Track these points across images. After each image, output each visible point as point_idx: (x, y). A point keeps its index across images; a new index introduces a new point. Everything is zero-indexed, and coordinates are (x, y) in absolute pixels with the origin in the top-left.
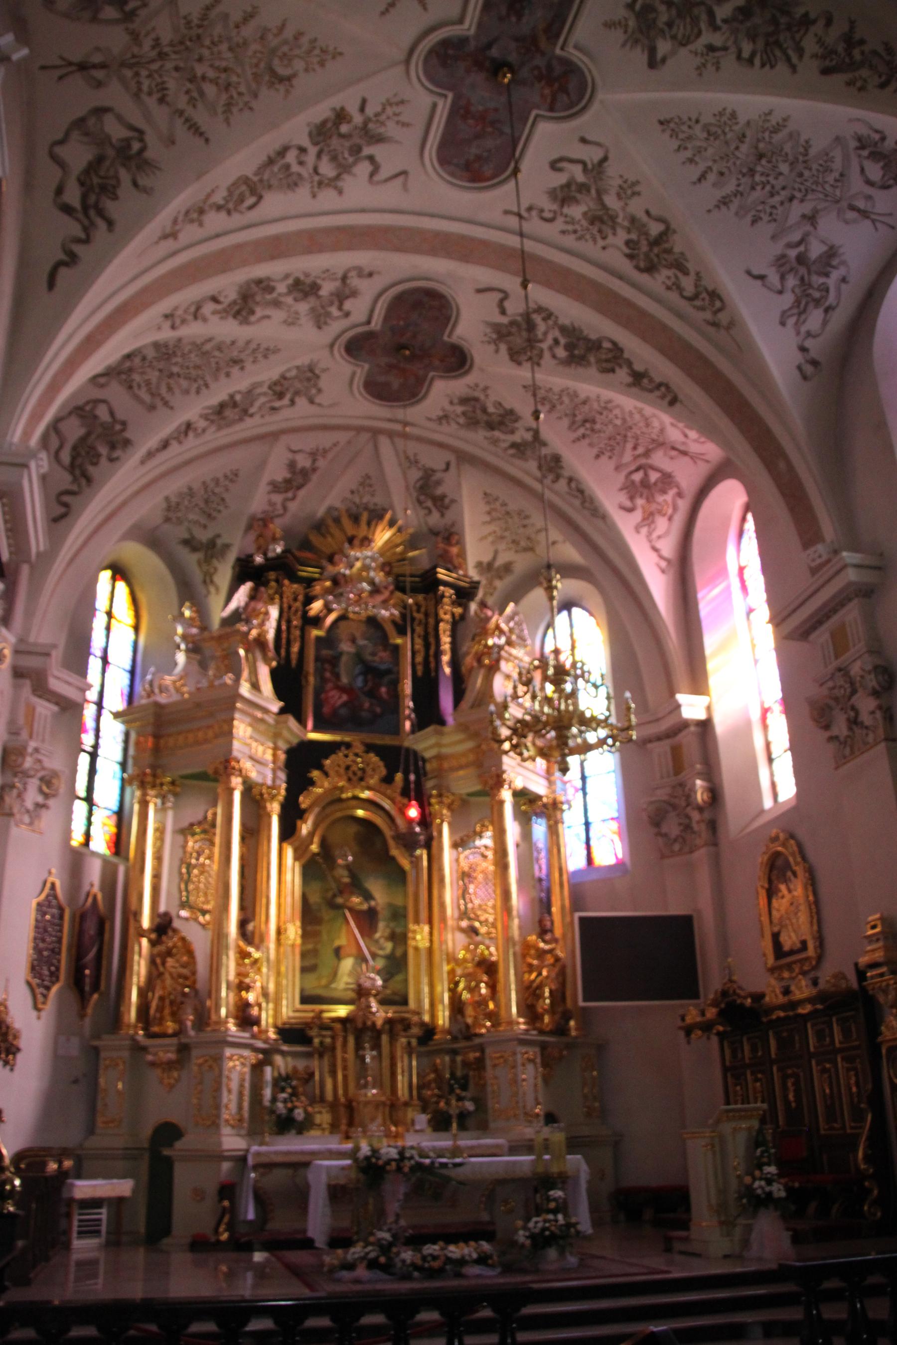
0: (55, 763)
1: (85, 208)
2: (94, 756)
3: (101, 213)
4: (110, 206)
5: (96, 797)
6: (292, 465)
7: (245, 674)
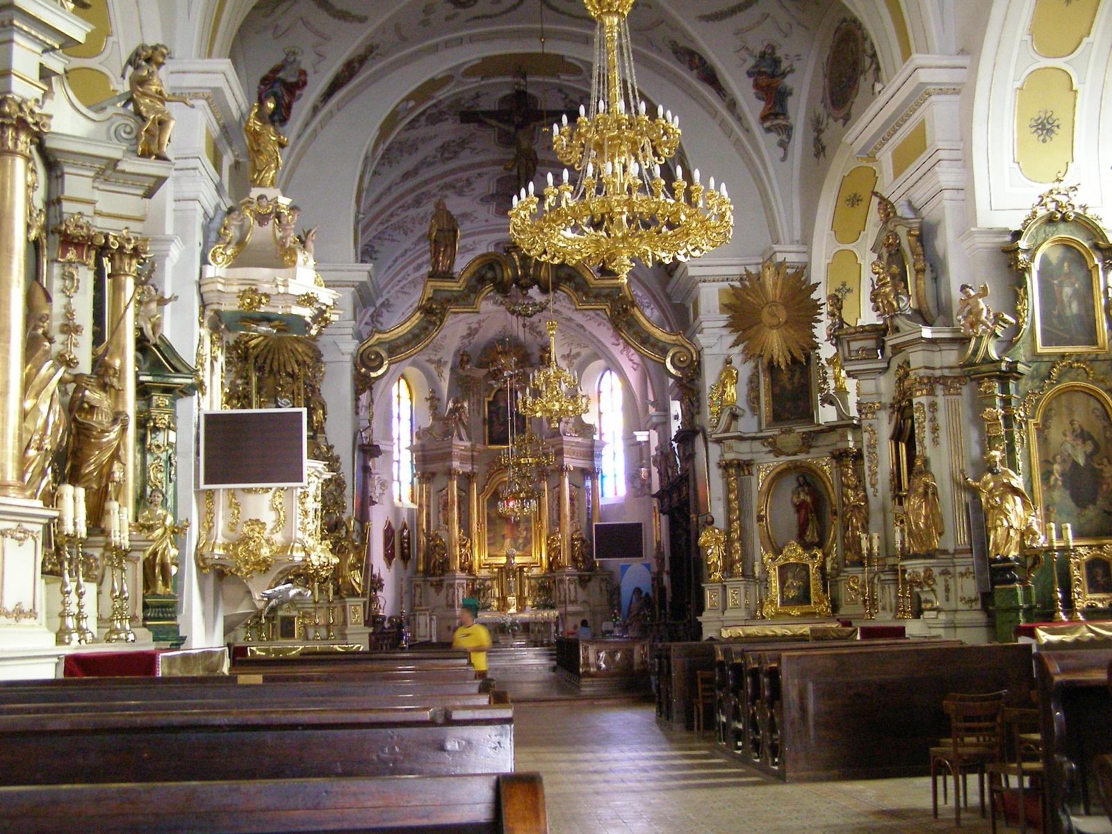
0: (384, 477)
1: (373, 322)
2: (398, 462)
3: (378, 322)
4: (380, 319)
5: (401, 479)
6: (470, 328)
7: (455, 433)
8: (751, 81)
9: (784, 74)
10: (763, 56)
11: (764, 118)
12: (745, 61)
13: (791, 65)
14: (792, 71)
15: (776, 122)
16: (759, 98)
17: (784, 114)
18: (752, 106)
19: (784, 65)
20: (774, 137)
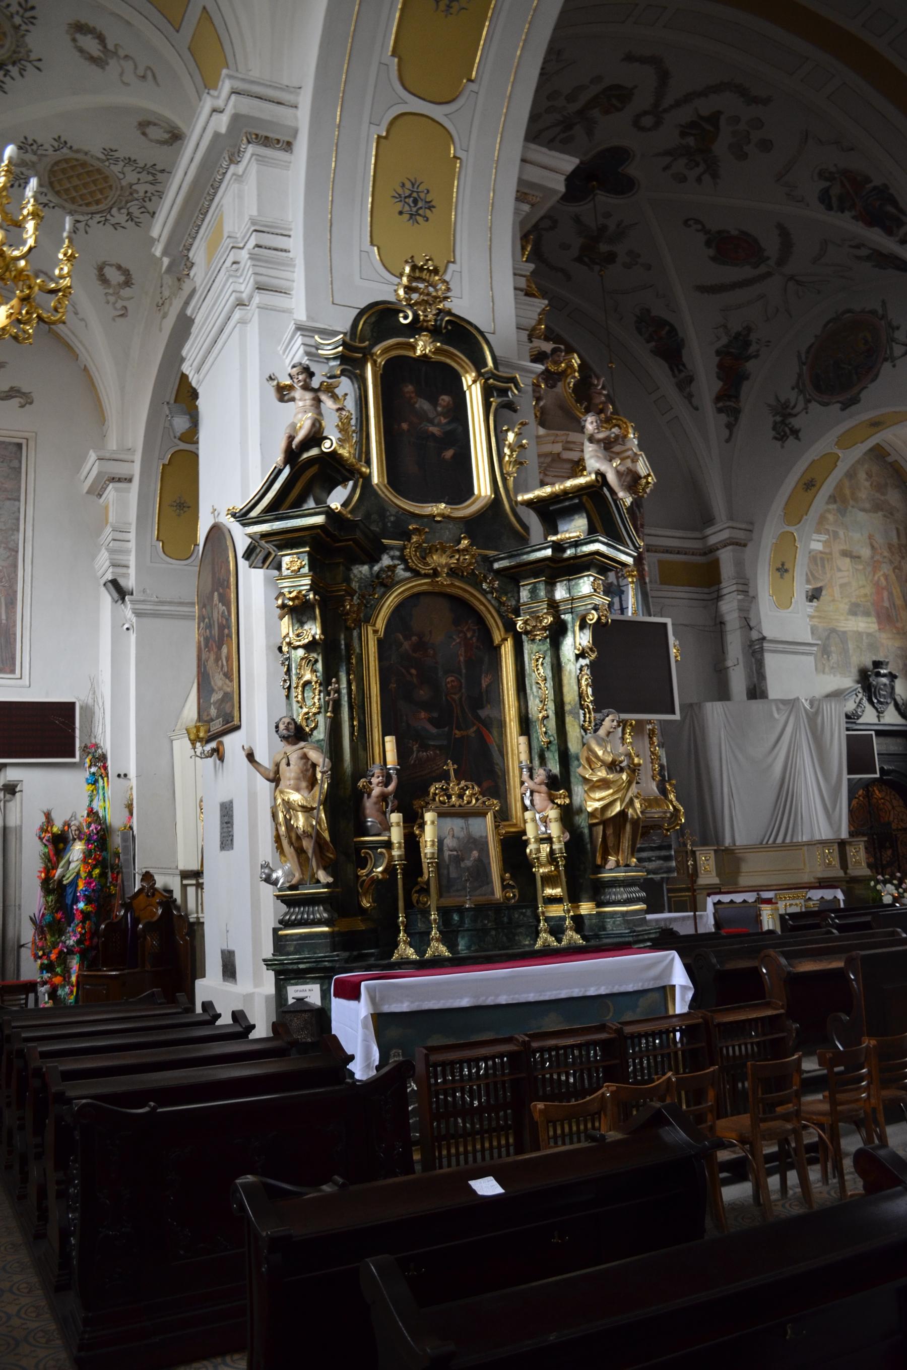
8: (717, 359)
9: (749, 358)
10: (738, 334)
11: (718, 399)
12: (719, 338)
13: (758, 351)
14: (756, 356)
15: (728, 403)
16: (719, 378)
17: (737, 397)
18: (707, 384)
19: (752, 349)
20: (723, 418)
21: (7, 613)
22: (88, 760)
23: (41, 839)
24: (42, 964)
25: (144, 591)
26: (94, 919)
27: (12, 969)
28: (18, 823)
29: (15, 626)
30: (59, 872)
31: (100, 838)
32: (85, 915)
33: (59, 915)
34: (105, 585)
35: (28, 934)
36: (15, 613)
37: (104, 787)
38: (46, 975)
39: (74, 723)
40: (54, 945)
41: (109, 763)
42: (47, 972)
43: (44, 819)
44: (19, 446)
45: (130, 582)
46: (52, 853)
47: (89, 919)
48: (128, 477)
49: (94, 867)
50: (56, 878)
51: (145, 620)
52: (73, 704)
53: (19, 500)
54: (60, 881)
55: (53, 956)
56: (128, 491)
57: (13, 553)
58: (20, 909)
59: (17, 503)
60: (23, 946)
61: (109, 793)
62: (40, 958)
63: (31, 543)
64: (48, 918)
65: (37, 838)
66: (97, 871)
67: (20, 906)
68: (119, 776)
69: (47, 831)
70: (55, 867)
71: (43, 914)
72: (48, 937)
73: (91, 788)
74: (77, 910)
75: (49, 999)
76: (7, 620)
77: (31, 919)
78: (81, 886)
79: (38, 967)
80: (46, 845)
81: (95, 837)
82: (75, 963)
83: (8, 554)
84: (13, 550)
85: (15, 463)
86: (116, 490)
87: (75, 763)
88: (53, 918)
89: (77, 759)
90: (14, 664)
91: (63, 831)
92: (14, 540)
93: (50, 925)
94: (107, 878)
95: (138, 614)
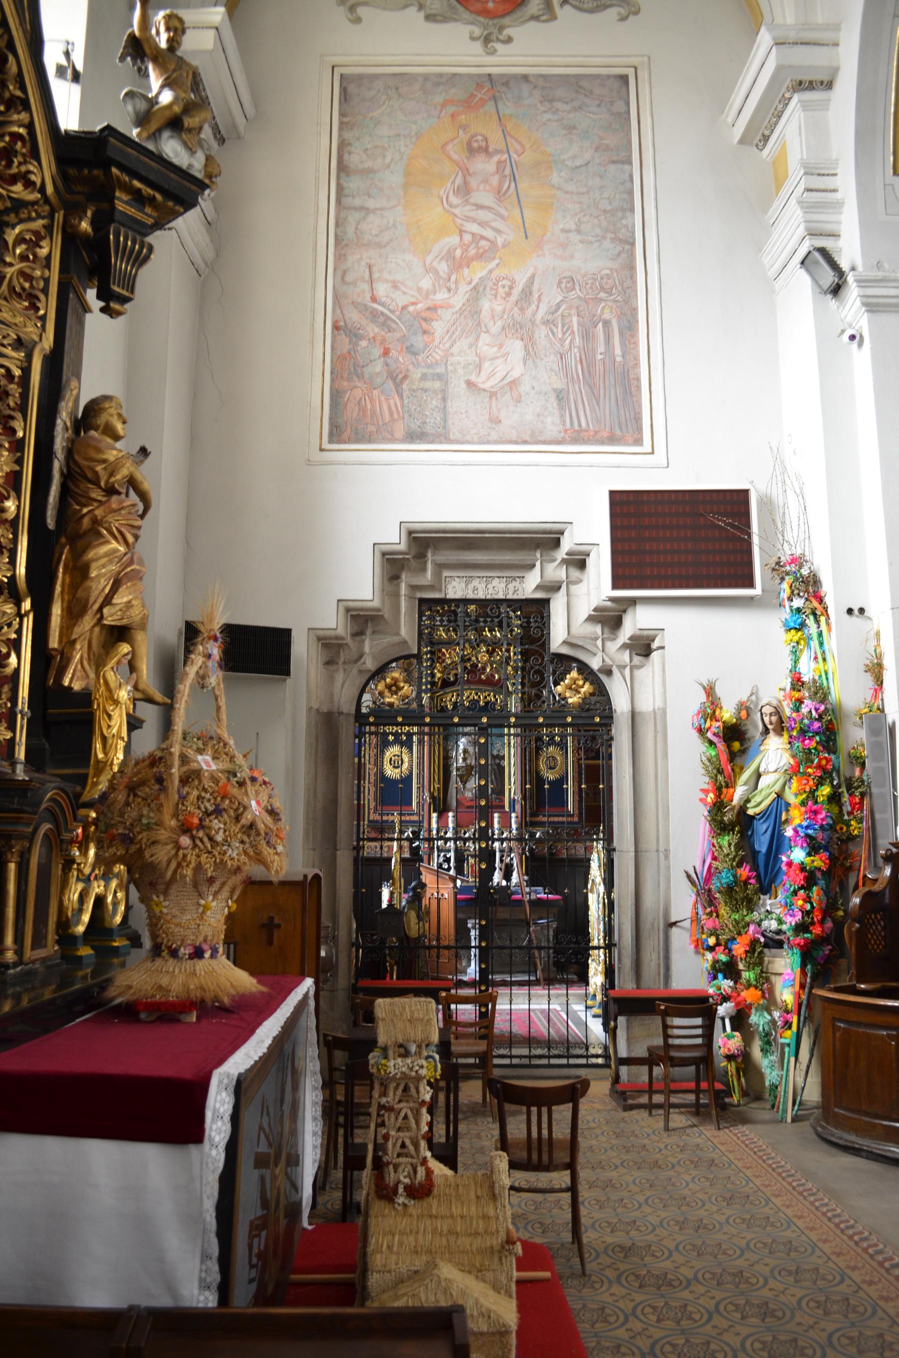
21: (623, 344)
22: (785, 586)
23: (701, 731)
24: (716, 962)
25: (879, 266)
26: (822, 883)
27: (654, 964)
28: (659, 704)
29: (637, 365)
30: (739, 793)
31: (820, 731)
32: (810, 878)
33: (744, 872)
34: (802, 263)
35: (683, 903)
36: (636, 344)
37: (820, 634)
38: (726, 984)
39: (748, 525)
40: (741, 927)
41: (828, 589)
42: (725, 977)
43: (703, 698)
44: (624, 79)
45: (850, 251)
46: (724, 757)
47: (816, 884)
48: (826, 79)
49: (820, 783)
50: (736, 801)
51: (886, 319)
52: (745, 493)
53: (630, 163)
54: (743, 809)
55: (739, 949)
56: (825, 106)
57: (627, 247)
58: (667, 857)
59: (627, 167)
60: (674, 924)
61: (832, 643)
62: (711, 949)
63: (654, 228)
64: (726, 878)
65: (695, 734)
66: (826, 790)
67: (667, 851)
68: (850, 611)
69: (713, 717)
70: (730, 784)
71: (710, 867)
72: (723, 910)
73: (795, 636)
74: (790, 864)
75: (734, 1029)
76: (623, 356)
77: (689, 876)
78: (797, 817)
79: (707, 965)
80: (711, 743)
81: (817, 725)
82: (786, 966)
83: (619, 248)
84: (626, 242)
85: (620, 106)
86: (805, 106)
87: (752, 598)
88: (735, 876)
89: (757, 591)
90: (640, 429)
91: (739, 718)
92: (626, 227)
93: (729, 891)
94: (840, 806)
95: (872, 307)
